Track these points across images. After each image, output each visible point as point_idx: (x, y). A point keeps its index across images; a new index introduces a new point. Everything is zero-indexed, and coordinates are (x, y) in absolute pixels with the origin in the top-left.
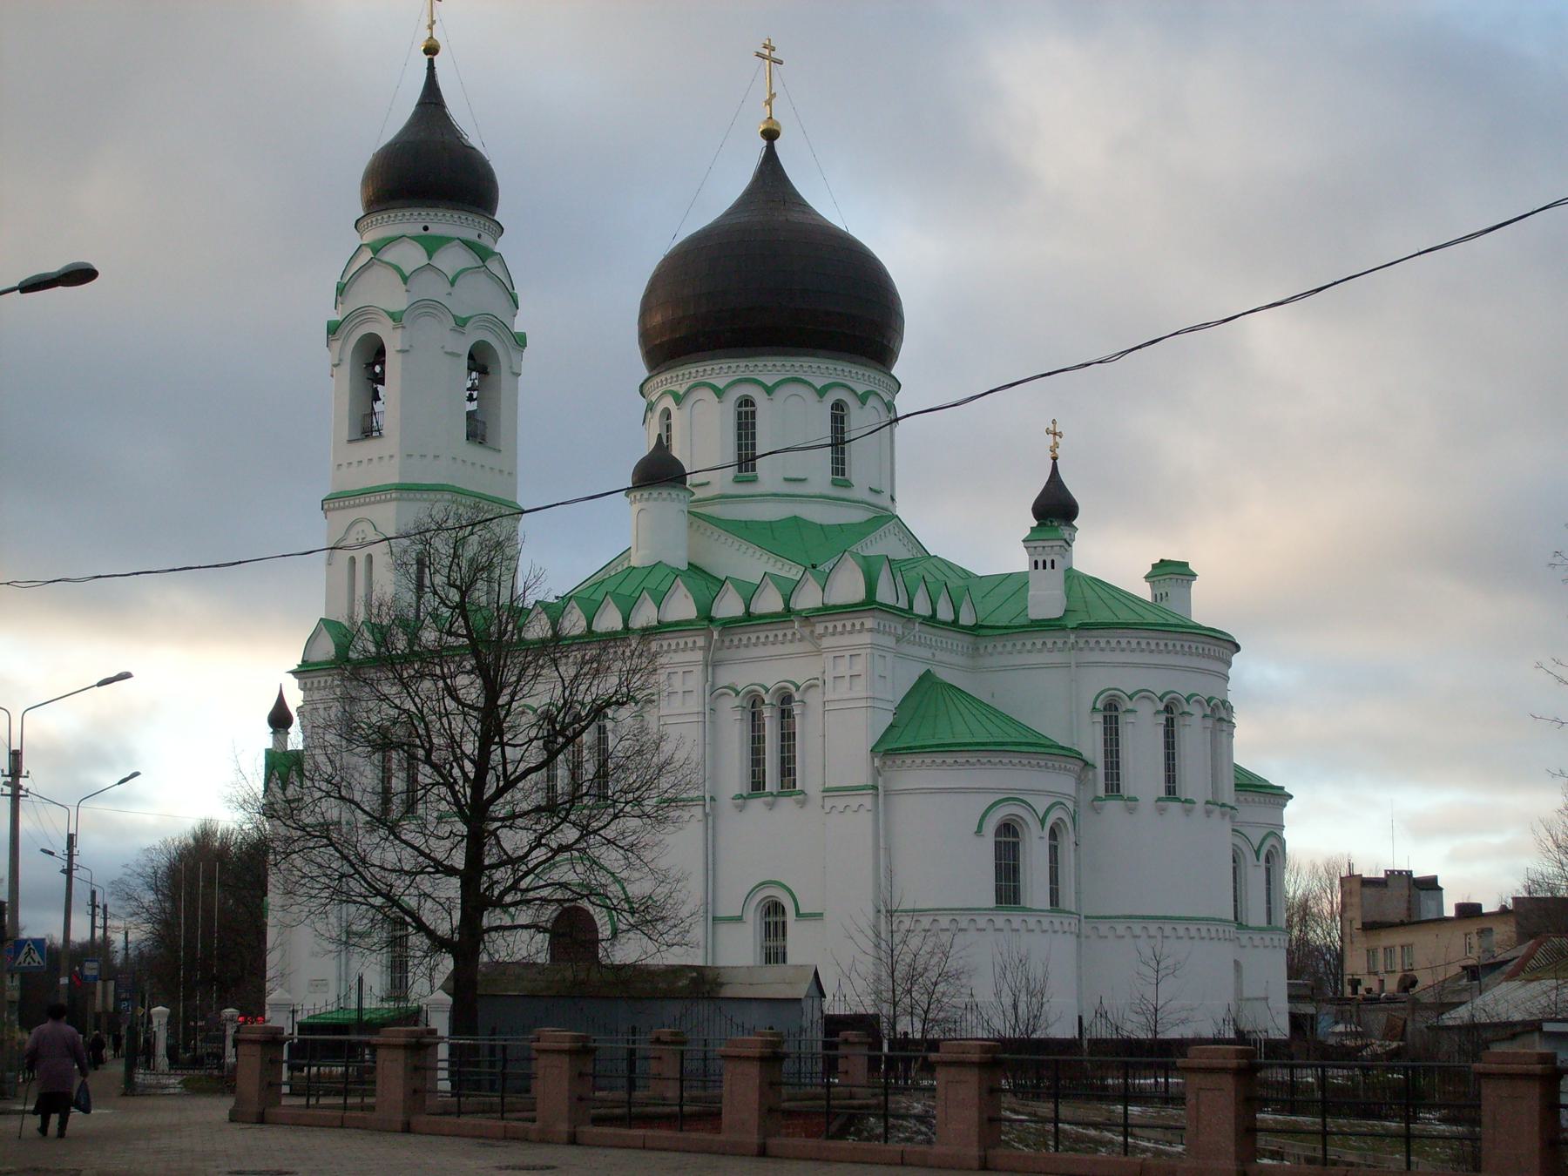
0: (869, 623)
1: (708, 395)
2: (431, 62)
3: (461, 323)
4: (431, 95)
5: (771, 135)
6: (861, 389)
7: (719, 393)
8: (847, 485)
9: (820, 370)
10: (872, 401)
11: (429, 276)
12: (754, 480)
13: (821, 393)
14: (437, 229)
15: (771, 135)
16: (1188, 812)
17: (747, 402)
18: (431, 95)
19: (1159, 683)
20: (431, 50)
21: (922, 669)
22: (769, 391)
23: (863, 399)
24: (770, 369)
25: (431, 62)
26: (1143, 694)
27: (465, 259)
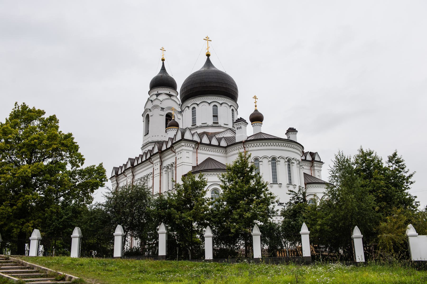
0: (183, 144)
1: (187, 108)
2: (163, 62)
3: (163, 109)
4: (163, 69)
5: (208, 55)
6: (221, 102)
7: (188, 107)
8: (217, 123)
9: (210, 99)
10: (223, 105)
11: (157, 100)
12: (195, 125)
13: (209, 104)
14: (160, 92)
15: (208, 55)
16: (280, 187)
17: (194, 108)
18: (163, 69)
19: (270, 154)
20: (163, 60)
21: (207, 157)
22: (198, 105)
23: (221, 104)
24: (198, 100)
25: (163, 62)
26: (265, 157)
27: (167, 97)
